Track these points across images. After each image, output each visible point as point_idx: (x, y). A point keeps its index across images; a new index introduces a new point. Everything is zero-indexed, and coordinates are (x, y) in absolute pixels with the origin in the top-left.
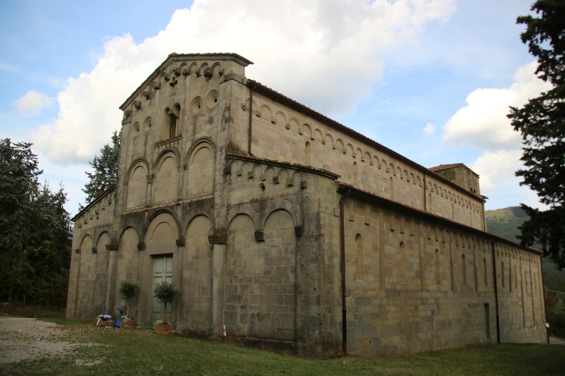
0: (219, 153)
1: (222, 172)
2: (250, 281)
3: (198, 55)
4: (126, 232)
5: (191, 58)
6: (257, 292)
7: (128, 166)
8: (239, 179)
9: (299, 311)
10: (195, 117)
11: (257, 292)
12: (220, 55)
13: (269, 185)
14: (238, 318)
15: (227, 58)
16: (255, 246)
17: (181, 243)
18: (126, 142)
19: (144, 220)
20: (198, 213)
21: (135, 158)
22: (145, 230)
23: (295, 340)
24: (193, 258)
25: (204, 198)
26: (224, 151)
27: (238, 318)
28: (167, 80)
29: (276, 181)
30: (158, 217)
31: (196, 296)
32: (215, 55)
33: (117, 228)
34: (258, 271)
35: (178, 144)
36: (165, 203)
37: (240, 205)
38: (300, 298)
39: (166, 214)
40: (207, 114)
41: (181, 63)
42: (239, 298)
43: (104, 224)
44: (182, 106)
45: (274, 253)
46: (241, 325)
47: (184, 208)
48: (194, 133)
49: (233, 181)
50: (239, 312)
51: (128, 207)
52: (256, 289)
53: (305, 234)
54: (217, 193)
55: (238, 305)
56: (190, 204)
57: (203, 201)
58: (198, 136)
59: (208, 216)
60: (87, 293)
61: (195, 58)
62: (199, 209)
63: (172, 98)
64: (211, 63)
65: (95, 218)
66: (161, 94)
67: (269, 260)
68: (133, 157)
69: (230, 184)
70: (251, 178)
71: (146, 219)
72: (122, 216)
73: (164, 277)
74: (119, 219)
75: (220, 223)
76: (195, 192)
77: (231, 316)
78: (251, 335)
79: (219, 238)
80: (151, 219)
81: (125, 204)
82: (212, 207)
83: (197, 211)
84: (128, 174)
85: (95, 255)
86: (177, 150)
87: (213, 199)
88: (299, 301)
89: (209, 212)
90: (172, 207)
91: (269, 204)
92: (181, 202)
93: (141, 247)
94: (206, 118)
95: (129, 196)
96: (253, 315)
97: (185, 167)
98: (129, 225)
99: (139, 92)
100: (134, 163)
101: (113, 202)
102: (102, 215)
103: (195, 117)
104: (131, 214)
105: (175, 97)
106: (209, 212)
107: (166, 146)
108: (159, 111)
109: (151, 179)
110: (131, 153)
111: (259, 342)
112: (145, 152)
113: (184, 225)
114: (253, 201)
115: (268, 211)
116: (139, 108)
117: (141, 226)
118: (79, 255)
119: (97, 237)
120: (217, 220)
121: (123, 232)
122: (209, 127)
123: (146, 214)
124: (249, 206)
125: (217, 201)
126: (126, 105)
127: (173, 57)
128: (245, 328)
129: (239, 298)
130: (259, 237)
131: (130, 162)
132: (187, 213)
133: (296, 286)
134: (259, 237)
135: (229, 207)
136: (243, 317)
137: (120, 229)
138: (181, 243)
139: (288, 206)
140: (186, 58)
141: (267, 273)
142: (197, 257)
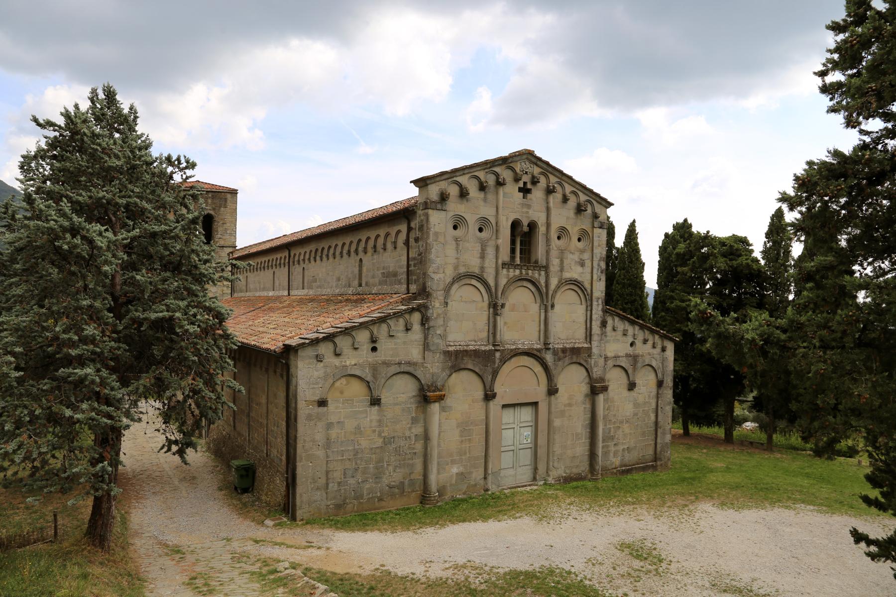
0: (595, 303)
1: (599, 323)
2: (622, 422)
3: (570, 178)
4: (454, 375)
5: (557, 174)
6: (627, 431)
7: (449, 280)
8: (614, 334)
9: (659, 440)
10: (562, 252)
11: (627, 431)
12: (597, 195)
13: (639, 343)
14: (612, 455)
15: (604, 203)
16: (626, 393)
17: (552, 391)
18: (441, 239)
19: (494, 363)
20: (574, 360)
21: (462, 270)
22: (495, 374)
23: (655, 460)
24: (565, 406)
25: (580, 346)
26: (600, 302)
27: (612, 455)
28: (517, 180)
29: (645, 341)
30: (513, 360)
31: (569, 443)
32: (591, 191)
33: (434, 367)
34: (628, 414)
35: (540, 275)
36: (524, 344)
37: (616, 357)
38: (659, 431)
39: (526, 357)
40: (577, 254)
41: (540, 170)
42: (612, 438)
43: (397, 360)
44: (542, 229)
45: (641, 399)
46: (614, 460)
47: (555, 352)
48: (562, 270)
49: (608, 334)
50: (612, 449)
51: (449, 339)
52: (626, 428)
53: (664, 385)
54: (595, 344)
55: (611, 444)
56: (564, 350)
57: (579, 349)
58: (567, 275)
59: (585, 364)
60: (356, 470)
61: (564, 178)
62: (574, 357)
63: (525, 210)
64: (583, 198)
65: (366, 347)
66: (504, 193)
67: (636, 405)
68: (456, 267)
69: (606, 336)
70: (625, 335)
71: (497, 361)
72: (447, 353)
73: (517, 429)
74: (438, 356)
75: (598, 373)
76: (563, 336)
77: (606, 454)
78: (621, 466)
79: (596, 388)
80: (504, 361)
81: (443, 337)
82: (590, 356)
83: (572, 358)
84: (447, 290)
85: (376, 407)
86: (539, 282)
87: (590, 349)
88: (659, 434)
89: (586, 361)
90: (539, 350)
91: (640, 360)
92: (551, 346)
93: (489, 396)
94: (576, 257)
95: (451, 324)
96: (623, 450)
97: (553, 306)
98: (463, 366)
99: (466, 171)
100: (458, 278)
101: (417, 327)
102: (385, 345)
103: (562, 252)
104: (466, 351)
105: (531, 212)
106: (586, 361)
107: (521, 273)
108: (504, 218)
109: (495, 308)
110: (452, 260)
111: (632, 469)
112: (482, 268)
113: (554, 372)
114: (628, 356)
115: (639, 365)
116: (463, 194)
117: (490, 369)
118: (325, 408)
119: (383, 381)
120: (595, 370)
121: (450, 376)
122: (580, 269)
123: (498, 355)
124: (624, 359)
125: (595, 350)
126: (438, 179)
127: (529, 156)
128: (616, 461)
129: (612, 438)
130: (632, 386)
131: (450, 273)
132: (559, 359)
133: (656, 423)
134: (632, 386)
135: (606, 358)
136: (615, 453)
137: (443, 370)
138: (552, 391)
139: (654, 364)
140: (550, 170)
141: (635, 414)
142: (570, 405)
